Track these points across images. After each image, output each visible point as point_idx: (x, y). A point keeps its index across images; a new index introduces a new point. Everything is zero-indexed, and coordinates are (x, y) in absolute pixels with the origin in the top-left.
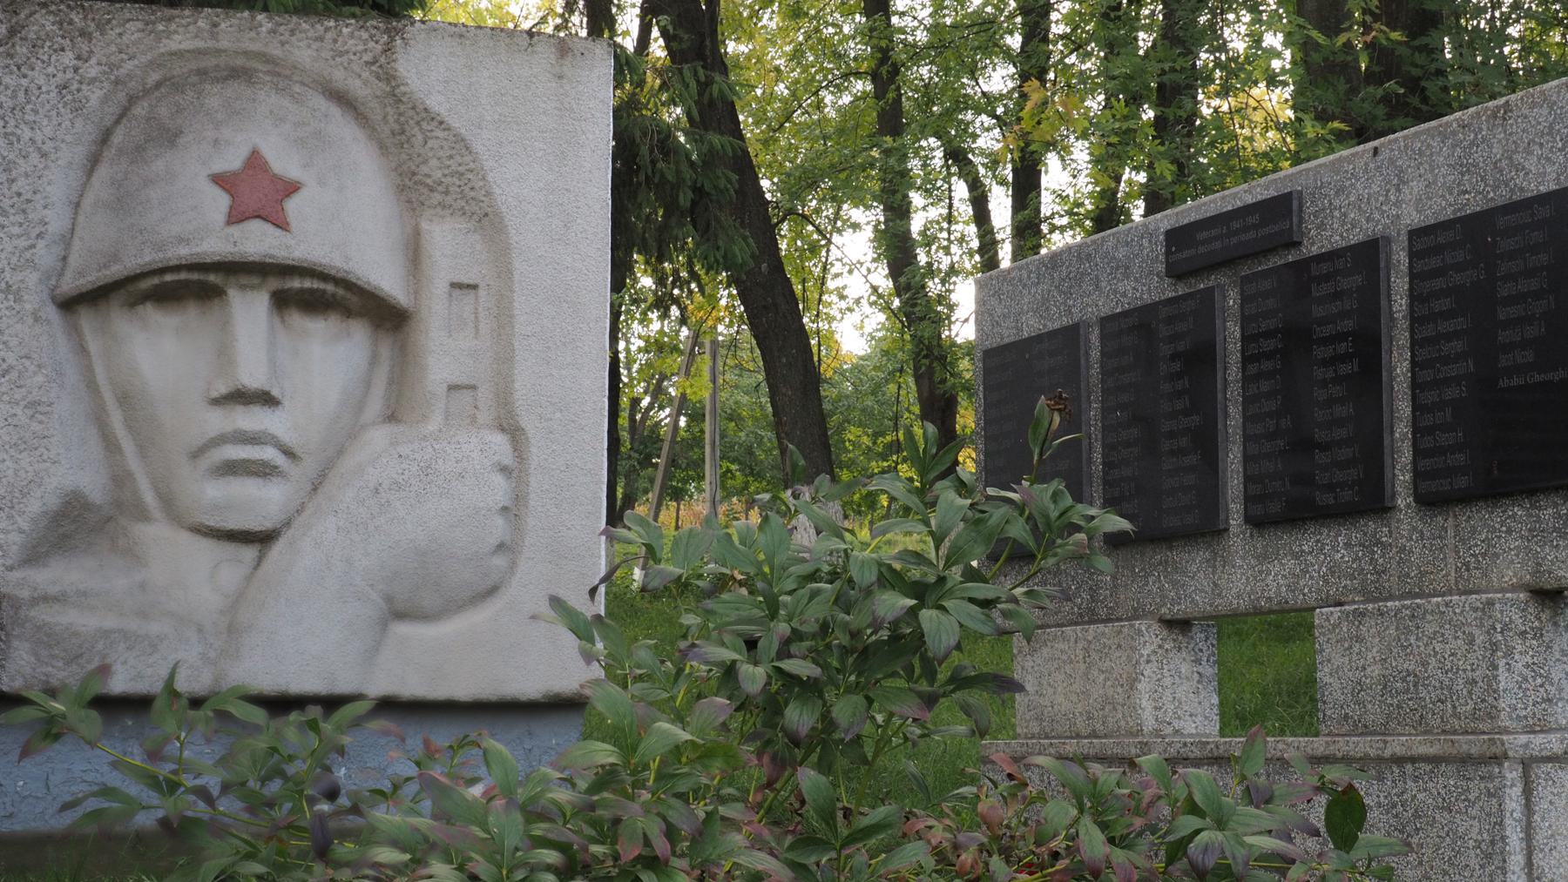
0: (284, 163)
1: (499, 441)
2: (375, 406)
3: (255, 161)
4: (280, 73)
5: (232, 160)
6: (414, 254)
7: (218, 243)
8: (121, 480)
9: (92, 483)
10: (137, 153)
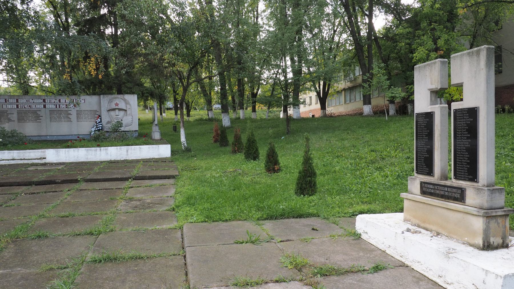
0: (118, 103)
1: (131, 117)
2: (125, 115)
3: (117, 103)
4: (118, 98)
5: (115, 103)
6: (126, 107)
7: (114, 108)
8: (111, 120)
9: (110, 120)
10: (110, 103)
